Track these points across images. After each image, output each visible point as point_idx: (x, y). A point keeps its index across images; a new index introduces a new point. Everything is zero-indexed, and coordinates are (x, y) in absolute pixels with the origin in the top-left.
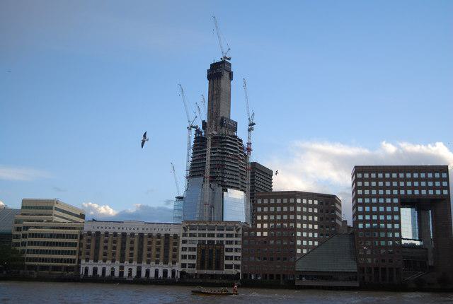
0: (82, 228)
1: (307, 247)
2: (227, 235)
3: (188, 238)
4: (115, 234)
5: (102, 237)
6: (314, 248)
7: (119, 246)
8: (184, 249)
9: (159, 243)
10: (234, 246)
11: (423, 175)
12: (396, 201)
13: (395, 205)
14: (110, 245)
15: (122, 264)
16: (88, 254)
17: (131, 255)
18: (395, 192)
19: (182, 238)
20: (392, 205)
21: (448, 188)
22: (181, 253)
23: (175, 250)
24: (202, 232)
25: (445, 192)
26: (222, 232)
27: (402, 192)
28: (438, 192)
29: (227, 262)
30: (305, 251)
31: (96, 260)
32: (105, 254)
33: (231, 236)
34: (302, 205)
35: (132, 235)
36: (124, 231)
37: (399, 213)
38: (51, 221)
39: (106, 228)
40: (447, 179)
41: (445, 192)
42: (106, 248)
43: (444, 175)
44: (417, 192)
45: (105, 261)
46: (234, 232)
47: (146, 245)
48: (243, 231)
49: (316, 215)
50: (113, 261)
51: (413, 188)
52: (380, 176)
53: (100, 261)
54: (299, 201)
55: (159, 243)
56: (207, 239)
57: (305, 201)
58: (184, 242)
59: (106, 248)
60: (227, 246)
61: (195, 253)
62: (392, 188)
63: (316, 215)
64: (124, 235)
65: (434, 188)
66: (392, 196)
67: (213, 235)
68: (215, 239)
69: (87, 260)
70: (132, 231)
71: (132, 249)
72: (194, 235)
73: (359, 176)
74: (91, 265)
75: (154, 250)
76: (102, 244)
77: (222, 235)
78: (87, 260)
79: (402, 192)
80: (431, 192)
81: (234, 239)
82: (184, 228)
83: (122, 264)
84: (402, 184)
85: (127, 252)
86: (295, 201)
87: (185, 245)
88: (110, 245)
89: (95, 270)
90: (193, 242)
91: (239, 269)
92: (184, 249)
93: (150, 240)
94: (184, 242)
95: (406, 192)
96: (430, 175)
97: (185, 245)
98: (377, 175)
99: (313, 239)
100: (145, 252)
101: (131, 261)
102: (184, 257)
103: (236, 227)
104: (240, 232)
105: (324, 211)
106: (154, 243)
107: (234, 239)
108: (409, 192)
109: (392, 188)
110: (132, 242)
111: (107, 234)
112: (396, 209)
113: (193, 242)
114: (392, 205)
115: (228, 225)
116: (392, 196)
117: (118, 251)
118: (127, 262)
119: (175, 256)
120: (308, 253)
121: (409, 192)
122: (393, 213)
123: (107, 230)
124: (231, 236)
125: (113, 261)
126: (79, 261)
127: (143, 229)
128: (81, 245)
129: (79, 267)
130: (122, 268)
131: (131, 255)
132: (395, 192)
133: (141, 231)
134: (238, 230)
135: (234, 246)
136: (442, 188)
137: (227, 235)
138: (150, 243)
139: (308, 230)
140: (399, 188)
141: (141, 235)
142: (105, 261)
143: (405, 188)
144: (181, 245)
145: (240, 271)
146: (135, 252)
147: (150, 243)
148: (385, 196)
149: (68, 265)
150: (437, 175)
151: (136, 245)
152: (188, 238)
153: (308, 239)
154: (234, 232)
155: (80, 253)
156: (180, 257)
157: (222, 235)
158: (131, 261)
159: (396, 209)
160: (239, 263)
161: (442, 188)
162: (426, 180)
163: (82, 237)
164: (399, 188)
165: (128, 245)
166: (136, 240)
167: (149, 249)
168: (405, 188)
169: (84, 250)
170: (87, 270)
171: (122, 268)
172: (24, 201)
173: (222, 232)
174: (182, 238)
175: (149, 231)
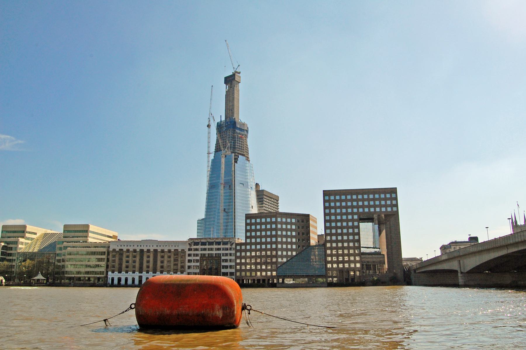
0: (109, 247)
1: (287, 256)
2: (223, 249)
3: (192, 252)
4: (135, 251)
5: (125, 253)
6: (292, 257)
7: (138, 259)
8: (190, 261)
9: (169, 257)
10: (228, 258)
11: (377, 196)
12: (356, 217)
13: (356, 220)
14: (131, 259)
15: (141, 274)
16: (114, 266)
17: (148, 267)
18: (355, 210)
19: (188, 252)
20: (353, 220)
21: (396, 205)
22: (187, 264)
23: (183, 262)
24: (203, 247)
25: (395, 209)
26: (219, 247)
27: (361, 210)
28: (389, 209)
29: (223, 270)
30: (285, 260)
31: (120, 272)
32: (127, 267)
33: (227, 249)
34: (282, 223)
35: (148, 251)
36: (142, 248)
37: (358, 227)
38: (86, 242)
39: (127, 246)
40: (396, 199)
41: (395, 209)
42: (127, 262)
43: (394, 196)
45: (127, 272)
46: (228, 246)
47: (159, 259)
49: (294, 230)
50: (134, 272)
53: (123, 272)
55: (169, 257)
56: (207, 252)
57: (284, 220)
58: (189, 255)
59: (127, 262)
60: (223, 258)
61: (198, 264)
62: (352, 207)
63: (294, 230)
64: (142, 251)
65: (386, 206)
66: (352, 214)
67: (212, 249)
68: (214, 252)
69: (113, 272)
70: (148, 248)
71: (148, 262)
72: (197, 250)
74: (116, 275)
75: (166, 262)
76: (124, 259)
77: (219, 249)
78: (113, 272)
79: (361, 210)
80: (383, 209)
81: (228, 252)
82: (189, 244)
83: (141, 274)
84: (360, 203)
85: (145, 264)
86: (276, 220)
87: (190, 258)
88: (131, 259)
89: (119, 280)
90: (197, 255)
92: (190, 261)
93: (162, 254)
94: (189, 255)
96: (382, 196)
97: (190, 258)
99: (292, 250)
100: (159, 264)
101: (148, 272)
102: (189, 267)
103: (231, 242)
104: (234, 246)
105: (301, 227)
106: (166, 257)
107: (228, 252)
108: (366, 210)
109: (352, 207)
110: (148, 257)
111: (128, 251)
112: (356, 224)
113: (197, 255)
114: (353, 220)
115: (224, 241)
116: (352, 214)
117: (137, 265)
118: (144, 273)
119: (183, 267)
120: (288, 261)
121: (366, 210)
122: (353, 227)
123: (128, 248)
124: (227, 249)
125: (134, 272)
126: (107, 274)
127: (157, 246)
128: (108, 260)
129: (107, 277)
130: (140, 278)
131: (148, 267)
132: (355, 210)
133: (155, 248)
134: (232, 245)
135: (228, 258)
136: (392, 206)
137: (223, 249)
138: (163, 257)
139: (287, 243)
140: (358, 207)
141: (156, 251)
142: (127, 272)
143: (363, 207)
144: (188, 258)
146: (151, 265)
147: (163, 257)
148: (347, 214)
149: (98, 276)
150: (388, 196)
151: (151, 259)
152: (192, 252)
153: (287, 250)
154: (228, 246)
155: (107, 266)
156: (187, 267)
157: (219, 249)
158: (148, 272)
159: (356, 224)
160: (233, 270)
161: (392, 206)
163: (108, 254)
164: (358, 207)
165: (145, 259)
166: (152, 255)
167: (162, 262)
168: (363, 207)
169: (110, 264)
170: (113, 279)
171: (140, 278)
172: (65, 226)
173: (219, 247)
174: (188, 252)
175: (162, 248)
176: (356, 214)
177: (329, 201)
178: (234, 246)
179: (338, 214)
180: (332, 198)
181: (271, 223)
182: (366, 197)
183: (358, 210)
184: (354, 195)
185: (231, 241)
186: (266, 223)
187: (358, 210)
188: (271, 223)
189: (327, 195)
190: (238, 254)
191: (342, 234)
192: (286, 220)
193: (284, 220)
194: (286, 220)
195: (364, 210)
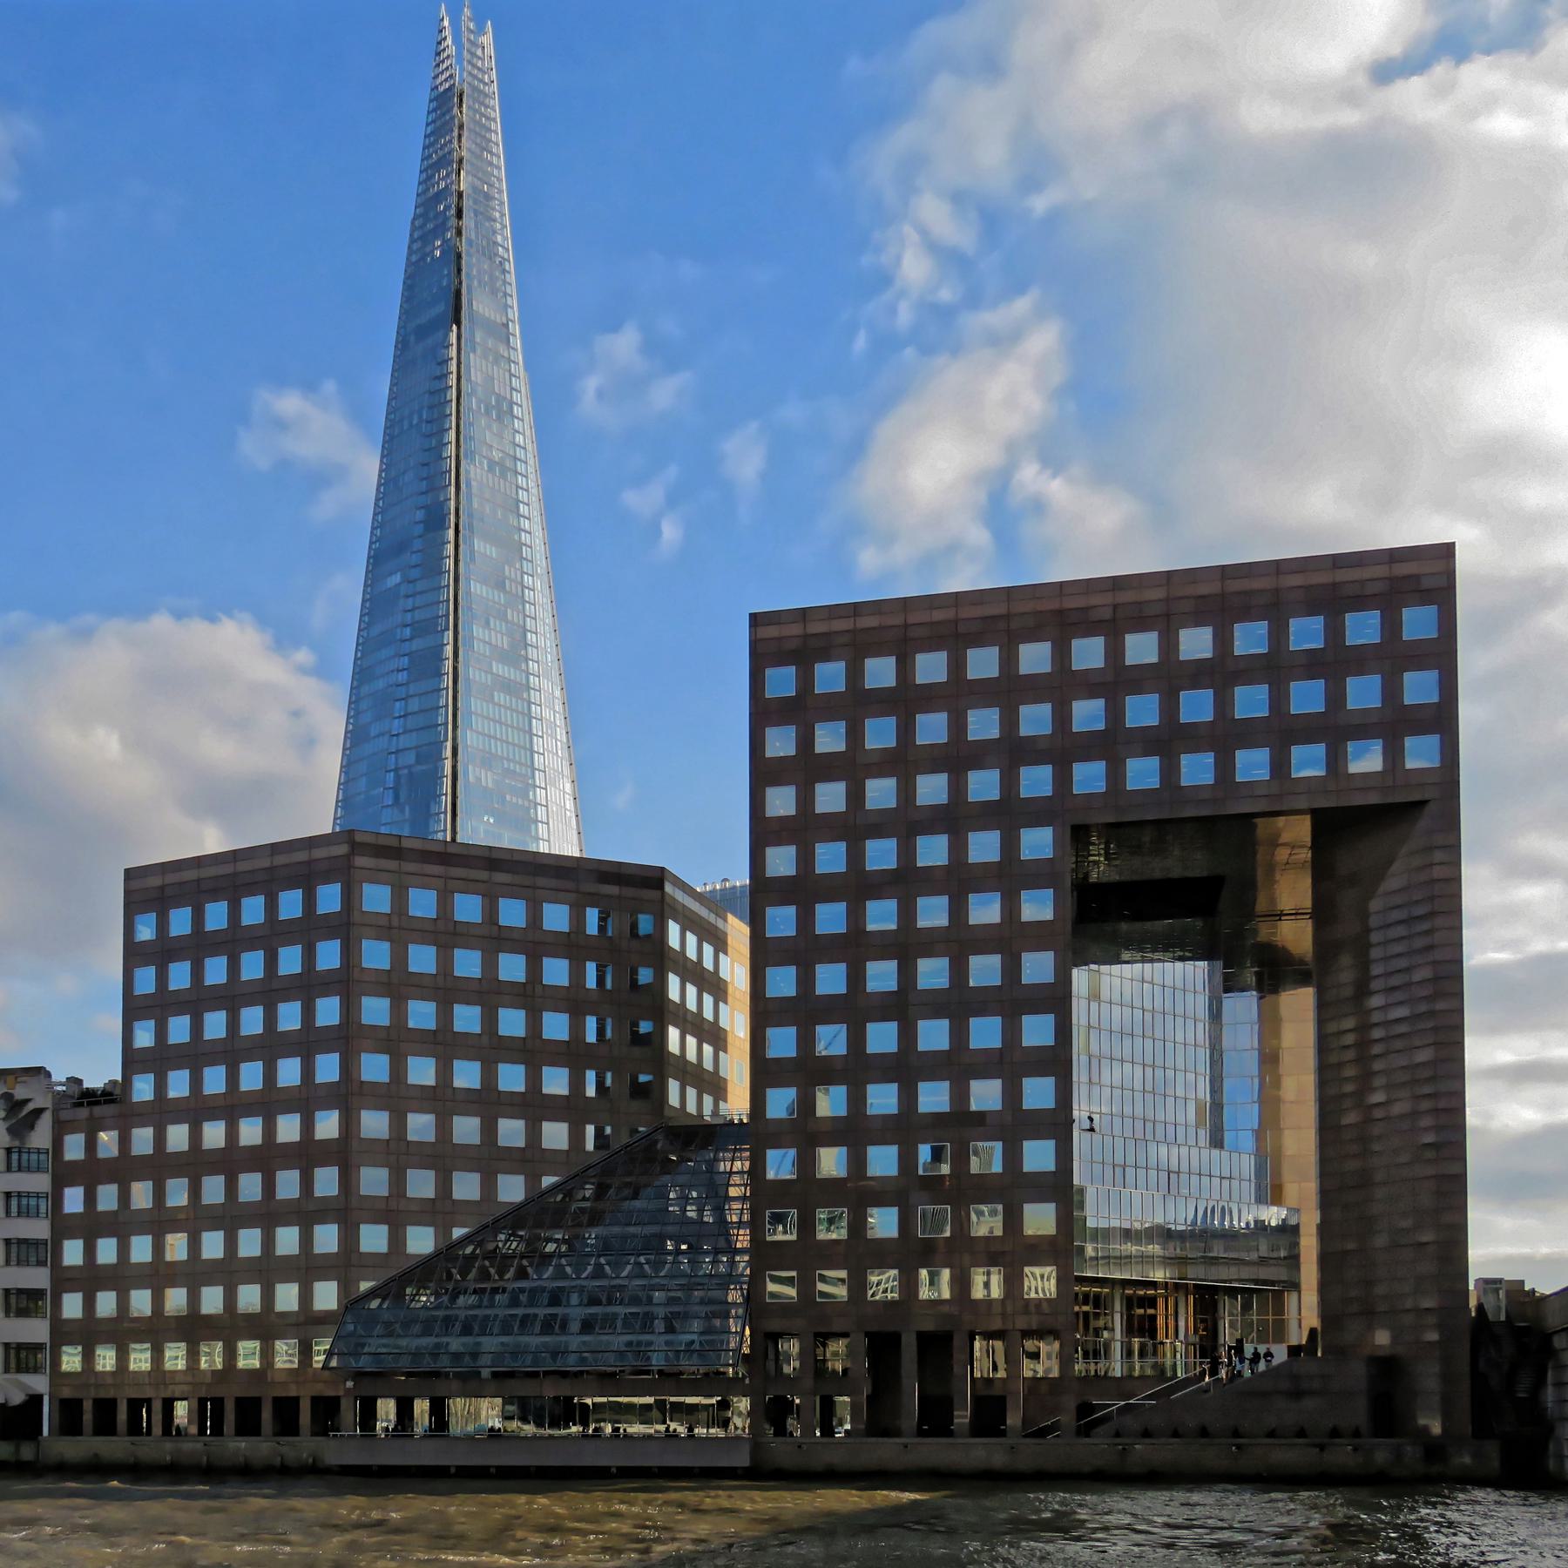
27: (1089, 777)
44: (1197, 769)
48: (60, 1130)
51: (1169, 740)
52: (931, 667)
54: (376, 898)
62: (1012, 752)
66: (1009, 814)
73: (782, 682)
91: (36, 1370)
95: (1116, 775)
98: (905, 669)
108: (1142, 773)
109: (1012, 752)
121: (1142, 773)
145: (39, 1383)
162: (1275, 668)
168: (1111, 744)
176: (1037, 813)
177: (801, 710)
178: (41, 1137)
179: (879, 825)
180: (830, 676)
181: (309, 930)
182: (1141, 648)
183: (1063, 779)
184: (1033, 636)
185: (20, 1093)
186: (271, 936)
187: (1063, 779)
188: (309, 930)
189: (781, 660)
190: (73, 1200)
191: (904, 1006)
192: (445, 904)
193: (423, 903)
194: (445, 904)
195: (1116, 775)
